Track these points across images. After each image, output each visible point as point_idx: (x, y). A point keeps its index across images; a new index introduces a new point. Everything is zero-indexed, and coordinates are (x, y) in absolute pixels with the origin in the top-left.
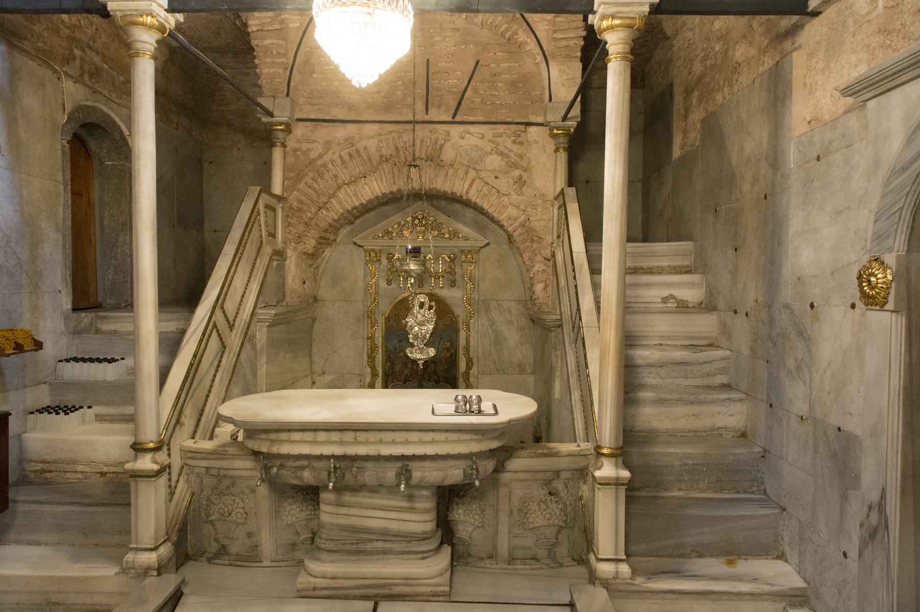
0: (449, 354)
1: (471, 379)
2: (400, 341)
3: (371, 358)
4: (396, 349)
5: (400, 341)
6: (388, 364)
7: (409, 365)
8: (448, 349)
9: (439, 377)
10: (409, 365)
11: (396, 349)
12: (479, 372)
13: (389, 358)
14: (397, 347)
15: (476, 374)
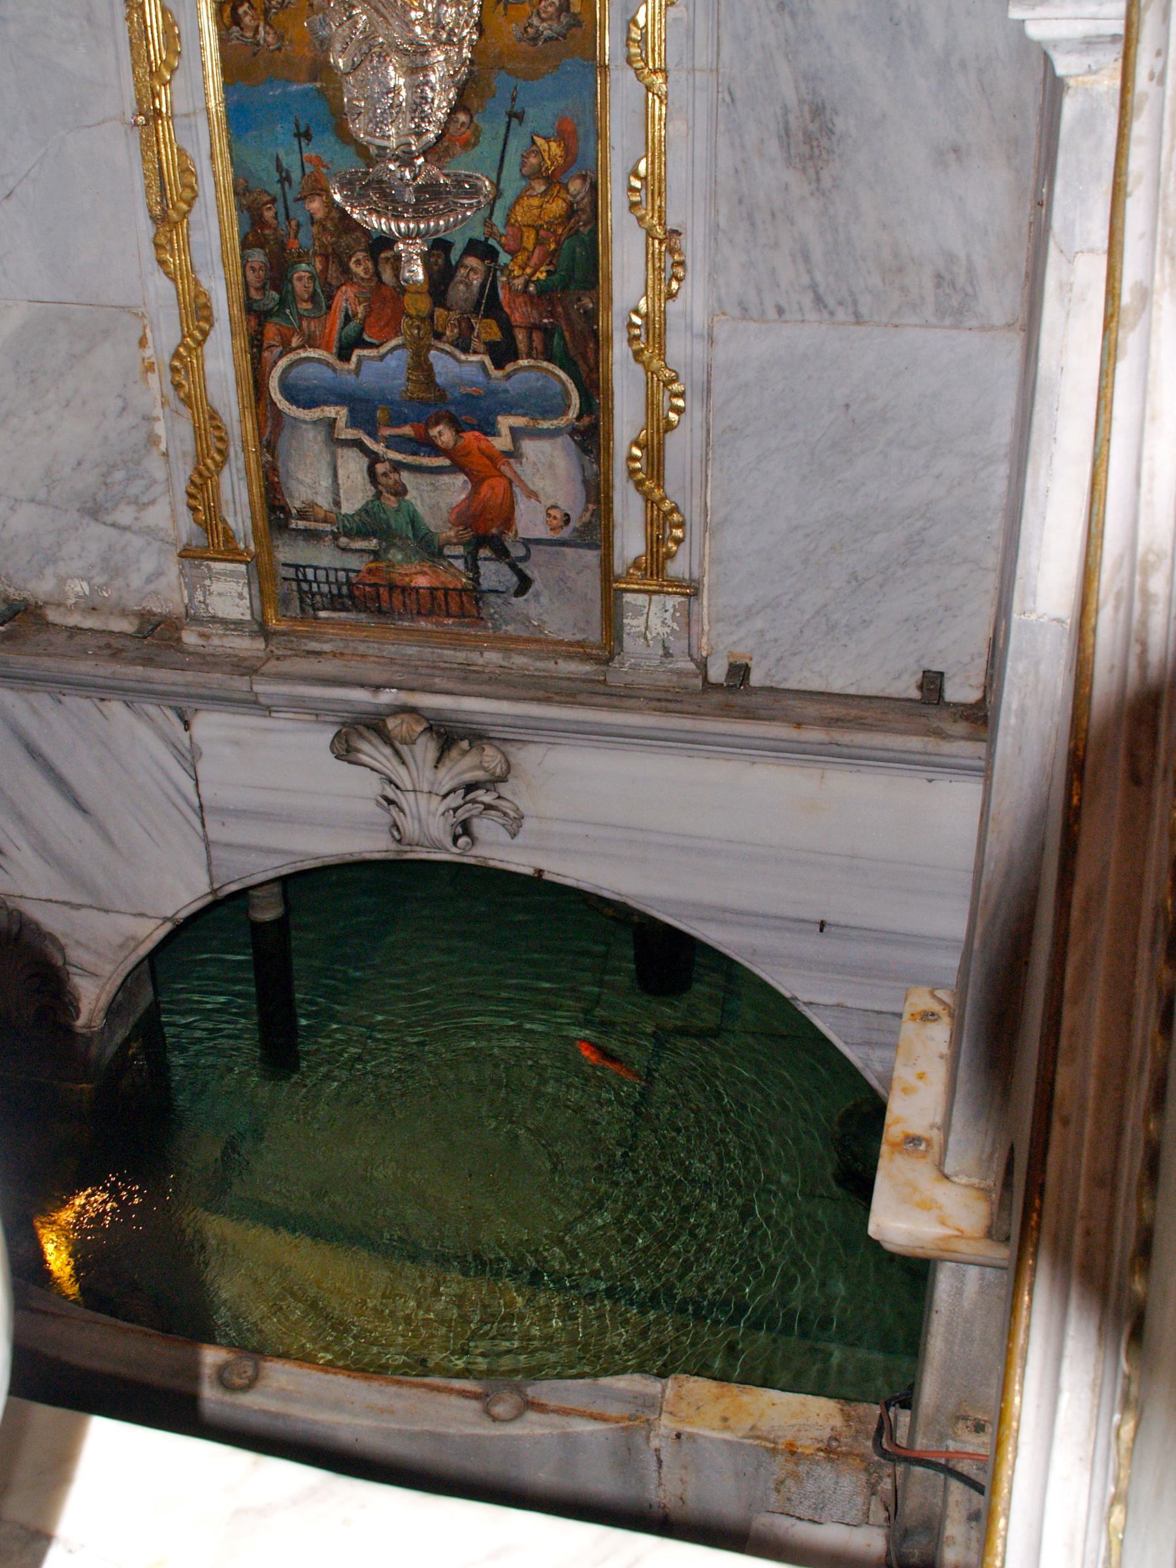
0: (556, 207)
1: (678, 348)
2: (304, 135)
3: (167, 220)
4: (285, 179)
5: (304, 135)
6: (258, 257)
7: (359, 267)
8: (553, 180)
9: (507, 328)
10: (359, 267)
11: (285, 179)
12: (718, 310)
13: (260, 227)
14: (292, 162)
15: (700, 319)
